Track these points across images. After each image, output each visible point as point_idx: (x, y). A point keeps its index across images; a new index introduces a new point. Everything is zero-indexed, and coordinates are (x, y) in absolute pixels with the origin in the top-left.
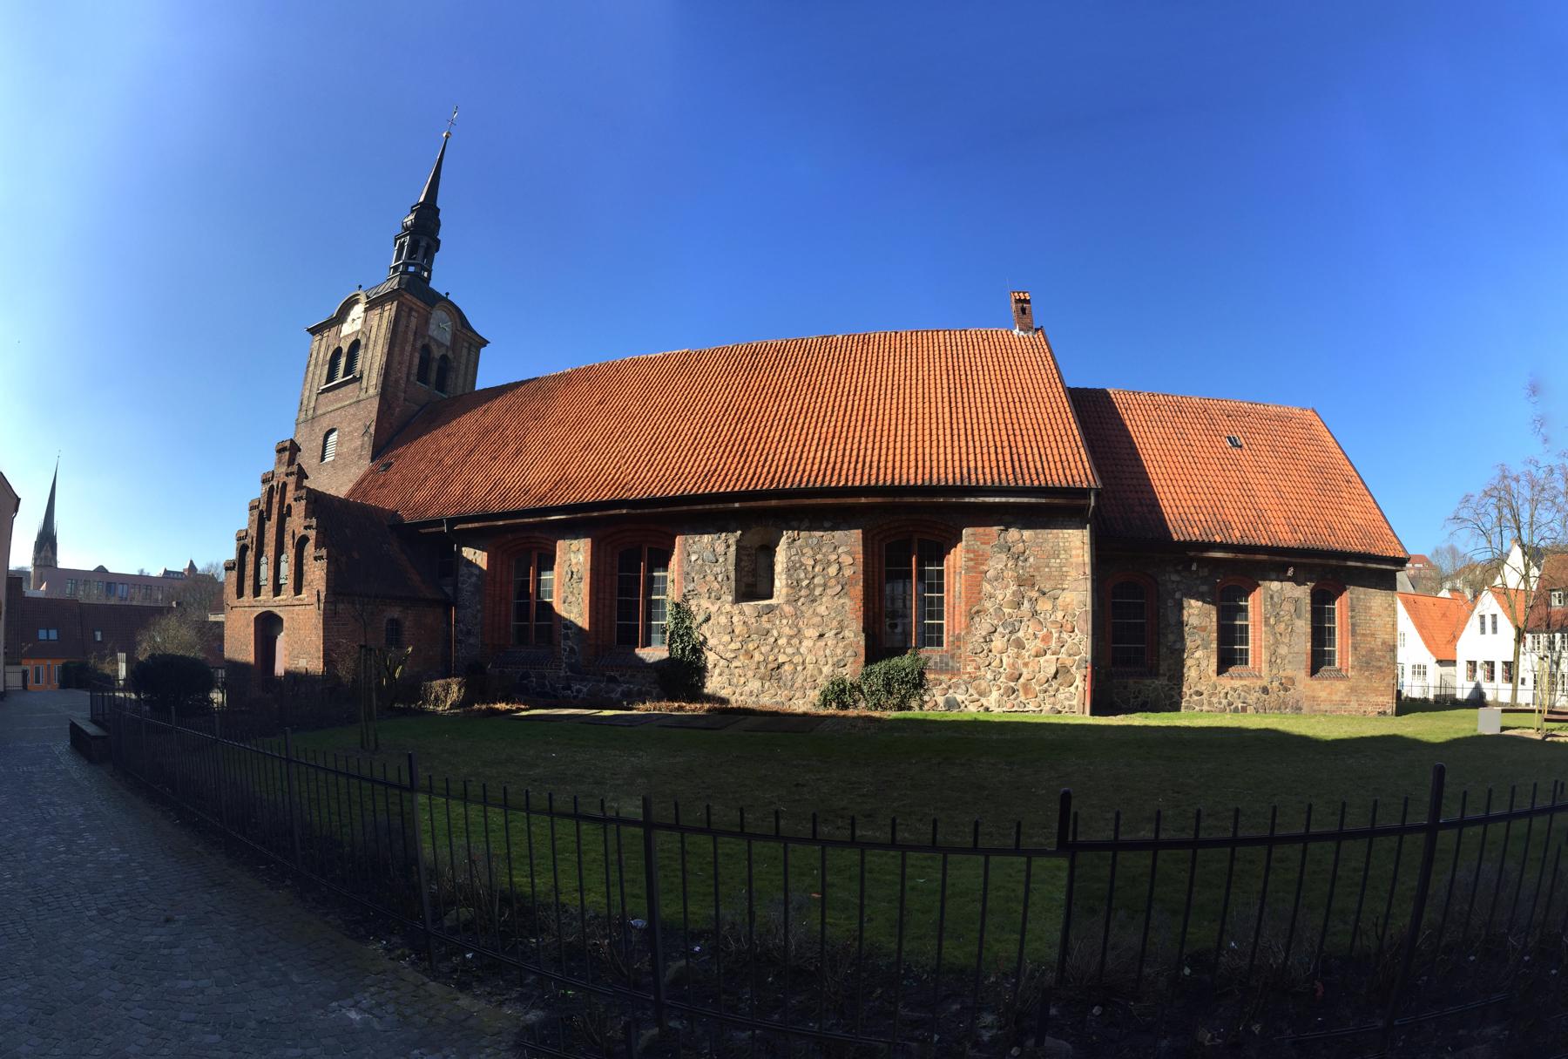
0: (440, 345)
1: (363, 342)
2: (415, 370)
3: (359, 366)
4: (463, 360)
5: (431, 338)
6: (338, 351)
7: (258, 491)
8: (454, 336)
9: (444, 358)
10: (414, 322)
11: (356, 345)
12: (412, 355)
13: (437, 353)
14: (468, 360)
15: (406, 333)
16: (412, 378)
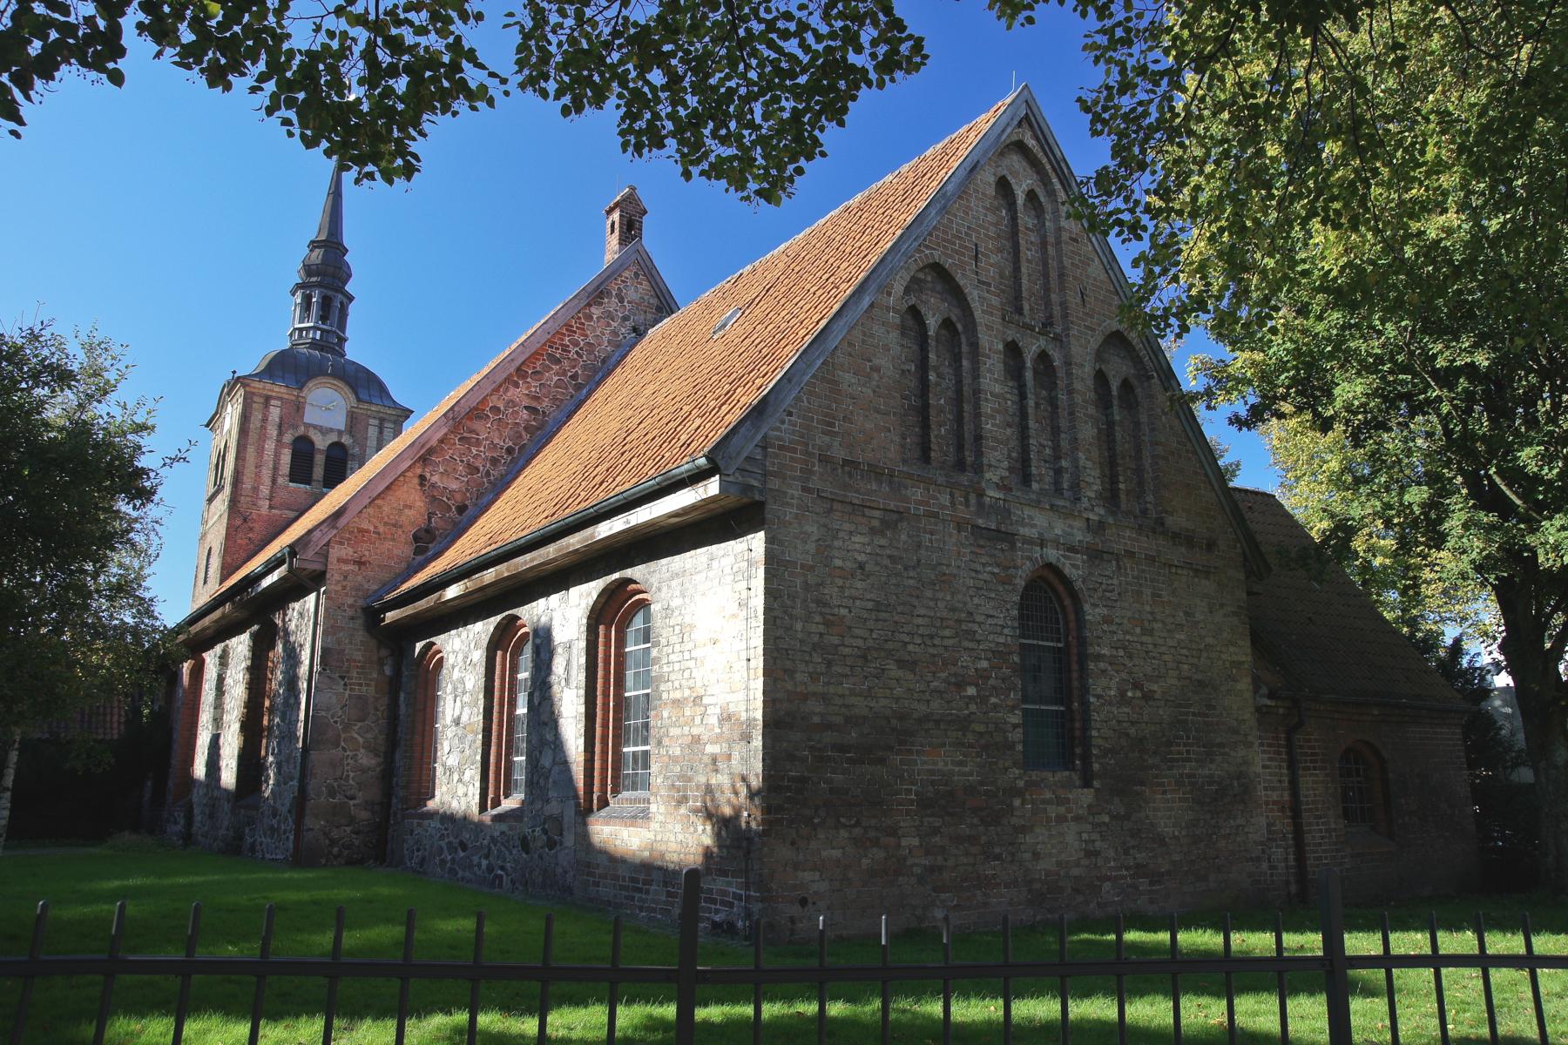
0: (324, 431)
2: (285, 468)
5: (308, 426)
6: (222, 457)
8: (352, 417)
9: (337, 446)
12: (277, 455)
13: (321, 443)
15: (263, 428)
16: (280, 480)
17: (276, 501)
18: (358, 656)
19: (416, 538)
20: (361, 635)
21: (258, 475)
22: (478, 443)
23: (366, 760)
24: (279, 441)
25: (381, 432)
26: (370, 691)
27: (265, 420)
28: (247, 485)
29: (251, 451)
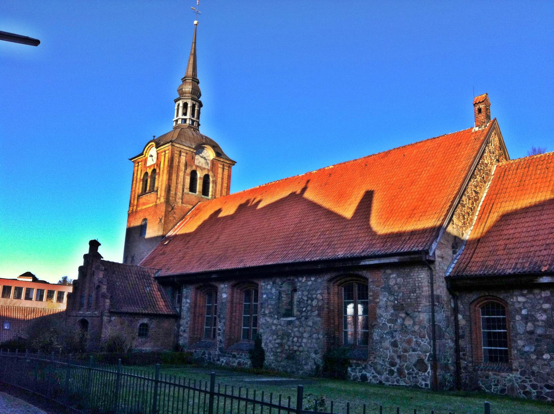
0: (202, 169)
1: (157, 171)
3: (156, 185)
4: (220, 176)
5: (197, 166)
7: (81, 263)
10: (183, 159)
11: (154, 171)
14: (223, 174)
15: (179, 165)
16: (186, 191)
17: (184, 200)
18: (445, 299)
19: (453, 247)
20: (445, 289)
21: (177, 188)
22: (465, 207)
23: (452, 344)
24: (185, 172)
25: (223, 171)
26: (449, 313)
27: (179, 162)
28: (173, 192)
29: (174, 177)
